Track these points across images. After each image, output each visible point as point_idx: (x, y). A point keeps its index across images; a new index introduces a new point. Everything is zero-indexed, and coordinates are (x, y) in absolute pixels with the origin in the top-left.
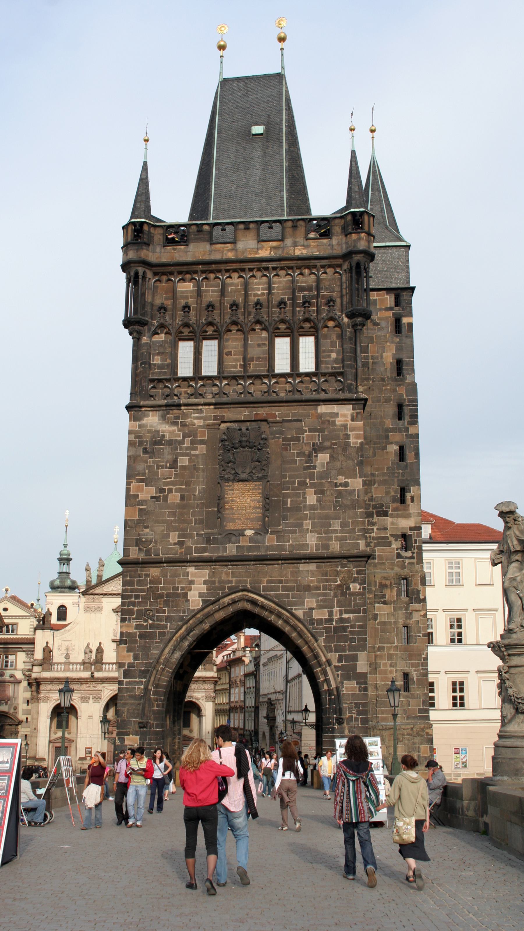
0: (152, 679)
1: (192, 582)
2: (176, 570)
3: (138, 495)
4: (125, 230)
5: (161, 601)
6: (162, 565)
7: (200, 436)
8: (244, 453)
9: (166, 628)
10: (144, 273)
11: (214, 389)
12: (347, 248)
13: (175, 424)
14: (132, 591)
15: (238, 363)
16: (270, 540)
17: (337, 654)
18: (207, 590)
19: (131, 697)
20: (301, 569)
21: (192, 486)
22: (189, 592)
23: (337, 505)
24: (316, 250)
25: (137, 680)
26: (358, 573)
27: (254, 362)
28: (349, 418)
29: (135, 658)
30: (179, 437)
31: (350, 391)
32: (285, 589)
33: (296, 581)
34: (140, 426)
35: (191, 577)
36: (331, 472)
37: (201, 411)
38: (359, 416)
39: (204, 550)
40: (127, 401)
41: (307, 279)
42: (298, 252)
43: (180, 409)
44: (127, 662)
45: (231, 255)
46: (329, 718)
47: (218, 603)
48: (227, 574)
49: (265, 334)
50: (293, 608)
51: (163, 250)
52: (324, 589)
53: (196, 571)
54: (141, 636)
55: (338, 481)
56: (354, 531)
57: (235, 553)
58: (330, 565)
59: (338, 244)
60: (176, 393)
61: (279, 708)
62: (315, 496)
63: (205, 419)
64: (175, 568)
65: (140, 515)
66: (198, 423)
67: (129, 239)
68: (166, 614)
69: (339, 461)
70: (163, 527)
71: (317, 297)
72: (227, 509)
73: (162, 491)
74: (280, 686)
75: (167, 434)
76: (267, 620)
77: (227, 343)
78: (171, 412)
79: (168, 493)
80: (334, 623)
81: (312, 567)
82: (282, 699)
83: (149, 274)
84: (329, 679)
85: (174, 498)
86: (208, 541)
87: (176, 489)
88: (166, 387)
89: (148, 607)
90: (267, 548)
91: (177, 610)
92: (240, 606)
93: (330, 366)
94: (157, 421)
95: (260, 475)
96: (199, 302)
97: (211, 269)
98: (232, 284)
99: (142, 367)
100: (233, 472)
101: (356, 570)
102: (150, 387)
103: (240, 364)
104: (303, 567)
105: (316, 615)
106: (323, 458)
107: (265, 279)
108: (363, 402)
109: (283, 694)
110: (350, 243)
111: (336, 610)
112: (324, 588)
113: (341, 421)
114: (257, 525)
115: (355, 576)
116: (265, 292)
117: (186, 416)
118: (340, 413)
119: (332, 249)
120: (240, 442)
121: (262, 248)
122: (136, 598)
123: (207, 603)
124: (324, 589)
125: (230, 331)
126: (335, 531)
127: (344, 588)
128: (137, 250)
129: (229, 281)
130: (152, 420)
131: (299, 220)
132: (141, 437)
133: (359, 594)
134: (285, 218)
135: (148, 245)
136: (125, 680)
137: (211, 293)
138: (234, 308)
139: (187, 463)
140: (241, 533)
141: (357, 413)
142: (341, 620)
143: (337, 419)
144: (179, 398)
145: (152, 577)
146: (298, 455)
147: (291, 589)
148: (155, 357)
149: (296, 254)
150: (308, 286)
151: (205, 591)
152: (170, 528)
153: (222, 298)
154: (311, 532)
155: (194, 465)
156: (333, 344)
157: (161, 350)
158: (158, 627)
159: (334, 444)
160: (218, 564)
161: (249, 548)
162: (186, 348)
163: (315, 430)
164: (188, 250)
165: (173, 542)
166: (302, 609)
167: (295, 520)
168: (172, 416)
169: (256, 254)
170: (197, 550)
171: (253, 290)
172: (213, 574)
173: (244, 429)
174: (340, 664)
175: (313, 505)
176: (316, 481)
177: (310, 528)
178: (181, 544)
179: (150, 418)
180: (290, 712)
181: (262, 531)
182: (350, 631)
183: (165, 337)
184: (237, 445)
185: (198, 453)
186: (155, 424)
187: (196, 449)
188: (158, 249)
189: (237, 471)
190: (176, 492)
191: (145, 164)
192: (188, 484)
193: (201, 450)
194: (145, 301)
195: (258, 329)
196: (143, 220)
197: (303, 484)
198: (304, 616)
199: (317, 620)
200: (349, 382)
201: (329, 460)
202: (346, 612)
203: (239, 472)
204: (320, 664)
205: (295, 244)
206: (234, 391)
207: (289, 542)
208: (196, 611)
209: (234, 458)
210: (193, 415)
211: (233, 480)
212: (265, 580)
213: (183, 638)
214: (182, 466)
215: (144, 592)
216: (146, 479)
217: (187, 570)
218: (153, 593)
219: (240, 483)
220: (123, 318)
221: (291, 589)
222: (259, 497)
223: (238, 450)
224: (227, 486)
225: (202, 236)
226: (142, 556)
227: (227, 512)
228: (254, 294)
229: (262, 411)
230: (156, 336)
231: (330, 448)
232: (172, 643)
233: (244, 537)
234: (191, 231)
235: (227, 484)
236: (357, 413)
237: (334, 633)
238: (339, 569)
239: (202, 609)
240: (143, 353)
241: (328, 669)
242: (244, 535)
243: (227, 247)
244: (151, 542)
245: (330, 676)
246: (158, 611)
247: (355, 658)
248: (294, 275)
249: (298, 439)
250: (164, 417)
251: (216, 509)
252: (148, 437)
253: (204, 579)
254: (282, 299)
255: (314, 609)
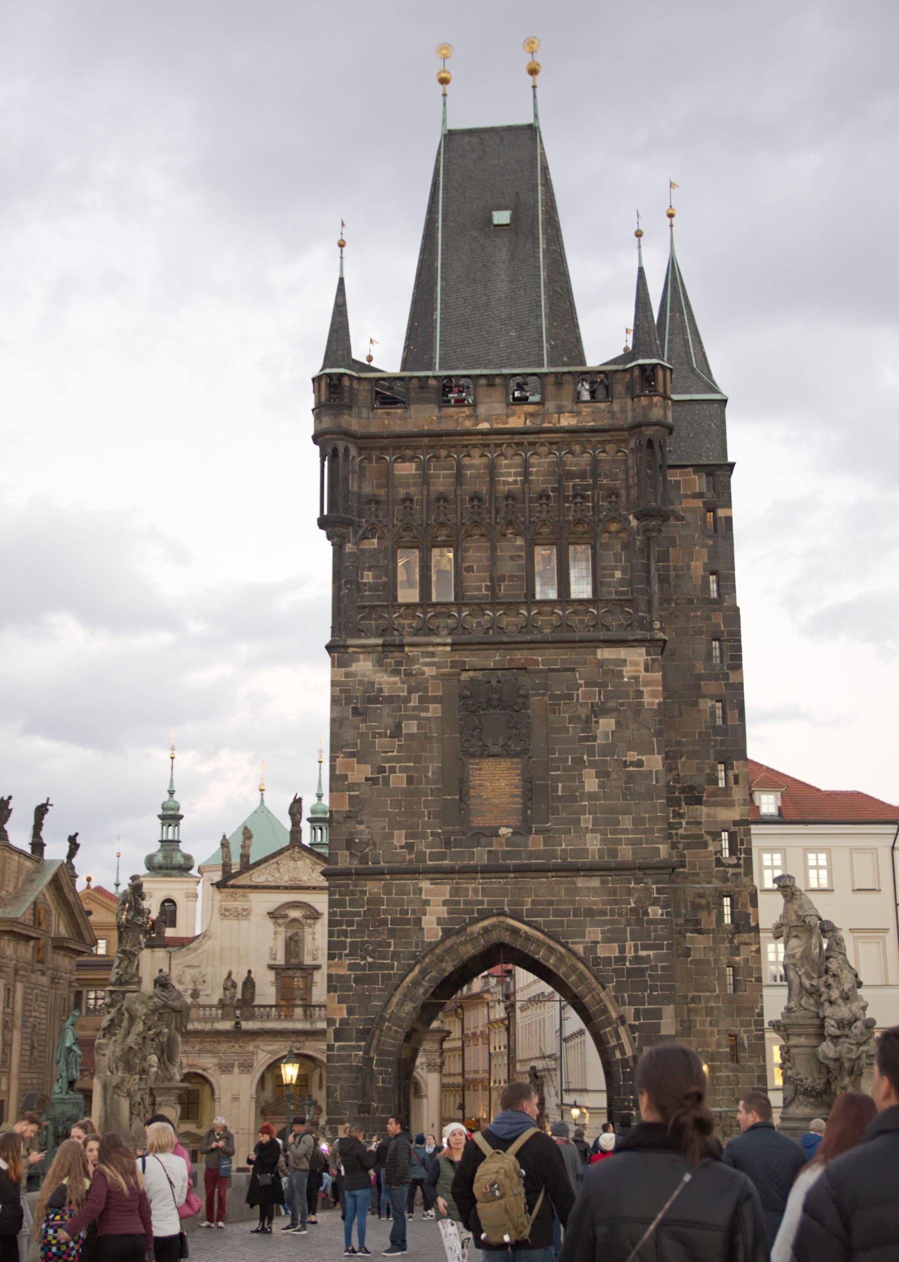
0: (375, 1042)
1: (427, 903)
2: (405, 885)
3: (345, 777)
4: (316, 384)
5: (383, 929)
6: (383, 877)
7: (433, 691)
9: (392, 969)
10: (346, 450)
11: (449, 621)
12: (634, 417)
13: (396, 672)
14: (343, 914)
15: (483, 584)
16: (536, 843)
17: (633, 1008)
18: (448, 913)
19: (345, 1067)
20: (579, 885)
21: (423, 764)
22: (423, 918)
23: (627, 793)
24: (590, 419)
25: (353, 1043)
26: (659, 891)
27: (506, 583)
28: (642, 668)
29: (350, 1011)
30: (403, 691)
31: (642, 627)
32: (557, 913)
33: (573, 902)
34: (347, 675)
35: (426, 895)
36: (617, 746)
37: (433, 655)
38: (656, 665)
39: (443, 856)
40: (327, 638)
41: (578, 461)
42: (567, 421)
43: (403, 651)
44: (338, 1018)
45: (468, 424)
46: (625, 1100)
47: (463, 933)
48: (475, 891)
49: (520, 542)
50: (570, 941)
51: (371, 415)
52: (612, 914)
53: (432, 886)
54: (358, 980)
55: (628, 759)
56: (651, 831)
57: (486, 862)
58: (620, 880)
59: (623, 411)
60: (395, 627)
61: (550, 1084)
62: (597, 780)
63: (438, 665)
64: (403, 881)
65: (351, 804)
66: (430, 671)
67: (323, 399)
68: (392, 948)
69: (629, 729)
70: (385, 823)
71: (594, 487)
72: (473, 796)
73: (381, 770)
74: (551, 1046)
75: (385, 687)
76: (532, 958)
77: (467, 554)
78: (390, 655)
79: (390, 772)
80: (627, 963)
81: (595, 883)
82: (555, 1069)
83: (353, 452)
84: (622, 1044)
85: (398, 780)
86: (448, 844)
87: (400, 767)
88: (381, 617)
89: (366, 939)
90: (531, 855)
91: (405, 943)
92: (495, 937)
93: (613, 590)
94: (370, 667)
95: (518, 749)
96: (425, 493)
97: (441, 443)
98: (472, 467)
99: (348, 589)
100: (480, 743)
101: (657, 888)
102: (359, 615)
103: (486, 586)
104: (581, 882)
105: (602, 952)
106: (607, 724)
107: (517, 460)
108: (661, 644)
109: (555, 1060)
110: (638, 410)
111: (629, 944)
112: (612, 913)
113: (630, 671)
114: (516, 820)
115: (656, 895)
116: (519, 478)
117: (411, 660)
118: (628, 659)
119: (613, 418)
120: (489, 700)
121: (513, 414)
122: (348, 926)
123: (447, 933)
124: (612, 914)
125: (471, 536)
126: (625, 831)
127: (639, 913)
128: (335, 416)
129: (466, 461)
130: (364, 666)
131: (564, 373)
132: (348, 691)
133: (661, 922)
134: (545, 370)
135: (350, 407)
136: (337, 1044)
137: (442, 482)
138: (475, 503)
139: (416, 731)
140: (494, 833)
141: (653, 660)
142: (637, 959)
143: (625, 669)
144: (401, 635)
145: (370, 894)
146: (572, 719)
147: (566, 913)
148: (365, 573)
149: (562, 425)
150: (579, 470)
151: (446, 916)
152: (395, 825)
153: (459, 487)
154: (592, 831)
155: (426, 733)
156: (617, 558)
157: (374, 563)
158: (382, 967)
159: (622, 705)
160: (462, 876)
161: (506, 855)
162: (407, 563)
163: (595, 684)
164: (408, 415)
165: (398, 844)
166: (581, 943)
167: (569, 814)
168: (393, 661)
169: (506, 423)
170: (433, 857)
171: (502, 475)
172: (455, 892)
173: (494, 683)
174: (637, 1023)
175: (594, 792)
176: (597, 758)
177: (590, 827)
178: (409, 847)
179: (361, 663)
180: (568, 1091)
181: (523, 830)
182: (650, 976)
183: (378, 543)
184: (485, 705)
185: (430, 715)
186: (368, 673)
187: (427, 710)
188: (365, 414)
190: (400, 772)
191: (341, 281)
192: (417, 760)
193: (434, 710)
194: (348, 491)
195: (511, 533)
196: (342, 370)
197: (578, 762)
198: (585, 953)
199: (604, 958)
200: (640, 614)
201: (614, 728)
202: (644, 948)
203: (490, 744)
204: (609, 1022)
205: (560, 411)
206: (479, 624)
207: (561, 845)
208: (433, 945)
209: (480, 723)
210: (421, 660)
211: (481, 756)
212: (530, 900)
213: (416, 983)
214: (408, 734)
215: (360, 916)
216: (358, 752)
217: (420, 886)
218: (373, 917)
219: (491, 759)
220: (318, 515)
221: (566, 913)
222: (517, 780)
223: (487, 712)
224: (472, 765)
225: (427, 395)
226: (355, 865)
227: (472, 801)
228: (504, 481)
229: (520, 656)
230: (366, 541)
231: (616, 710)
232: (401, 990)
233: (499, 838)
234: (411, 386)
235: (472, 761)
236: (653, 660)
237: (628, 978)
238: (632, 885)
239: (443, 941)
240: (348, 567)
241: (622, 1030)
242: (497, 836)
243: (464, 412)
244: (367, 844)
245: (625, 1040)
246: (380, 944)
247: (658, 1014)
248: (560, 454)
249: (570, 697)
250: (380, 663)
251: (457, 797)
252: (359, 692)
253: (443, 898)
254: (543, 490)
255: (598, 942)
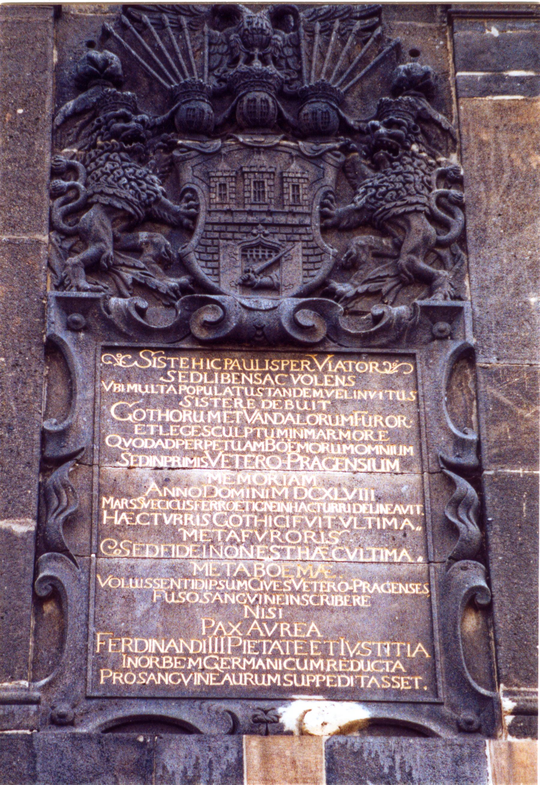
8: (262, 160)
189: (201, 270)
211: (176, 339)
227: (117, 552)
